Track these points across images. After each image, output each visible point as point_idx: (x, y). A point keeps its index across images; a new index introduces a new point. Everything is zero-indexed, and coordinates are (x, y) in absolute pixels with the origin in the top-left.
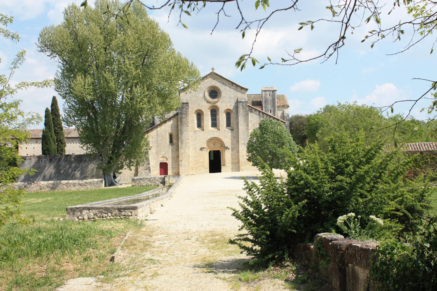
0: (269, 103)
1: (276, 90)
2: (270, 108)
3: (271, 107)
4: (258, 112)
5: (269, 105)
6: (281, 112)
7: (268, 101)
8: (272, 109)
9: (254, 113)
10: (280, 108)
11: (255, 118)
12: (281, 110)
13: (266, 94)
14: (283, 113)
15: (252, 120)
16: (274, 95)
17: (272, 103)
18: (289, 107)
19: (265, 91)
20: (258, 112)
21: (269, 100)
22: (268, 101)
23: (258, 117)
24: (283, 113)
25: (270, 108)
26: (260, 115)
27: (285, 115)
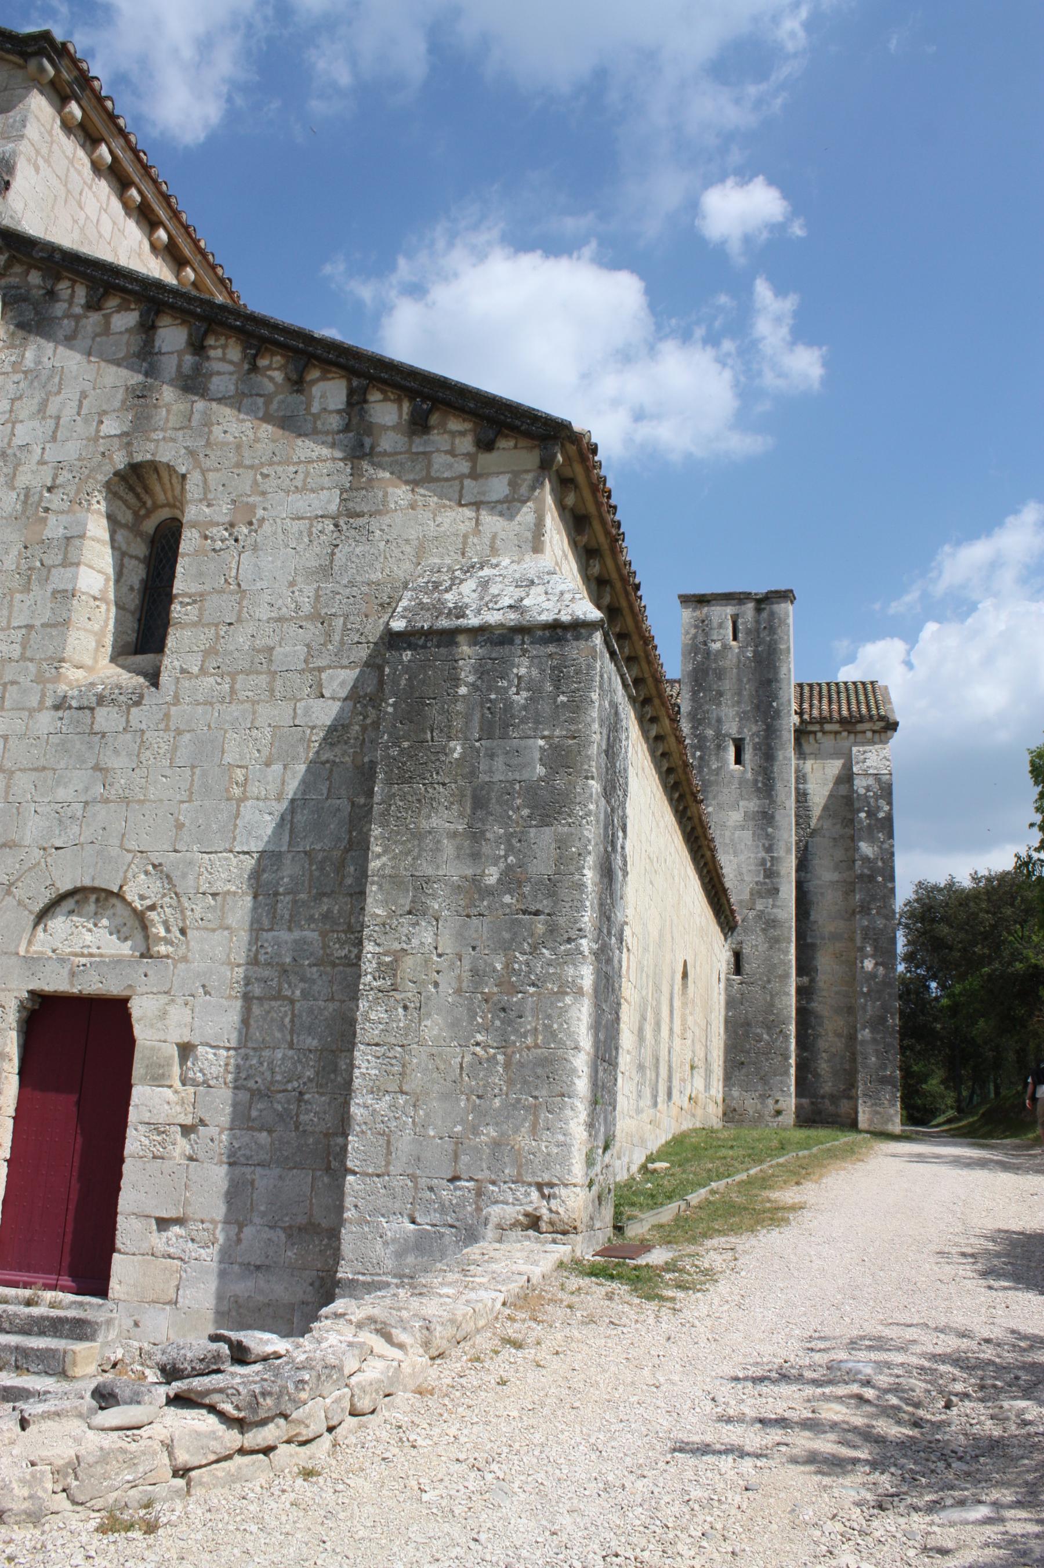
0: (728, 685)
1: (786, 595)
2: (731, 728)
3: (743, 717)
4: (125, 320)
5: (728, 699)
6: (834, 767)
7: (720, 674)
8: (750, 733)
9: (69, 341)
10: (828, 742)
11: (65, 404)
12: (835, 755)
13: (703, 626)
14: (846, 777)
15: (23, 433)
16: (771, 629)
17: (748, 688)
18: (893, 726)
19: (701, 600)
20: (125, 320)
21: (730, 661)
22: (720, 674)
23: (120, 378)
24: (846, 777)
25: (731, 728)
26: (145, 356)
27: (860, 784)
